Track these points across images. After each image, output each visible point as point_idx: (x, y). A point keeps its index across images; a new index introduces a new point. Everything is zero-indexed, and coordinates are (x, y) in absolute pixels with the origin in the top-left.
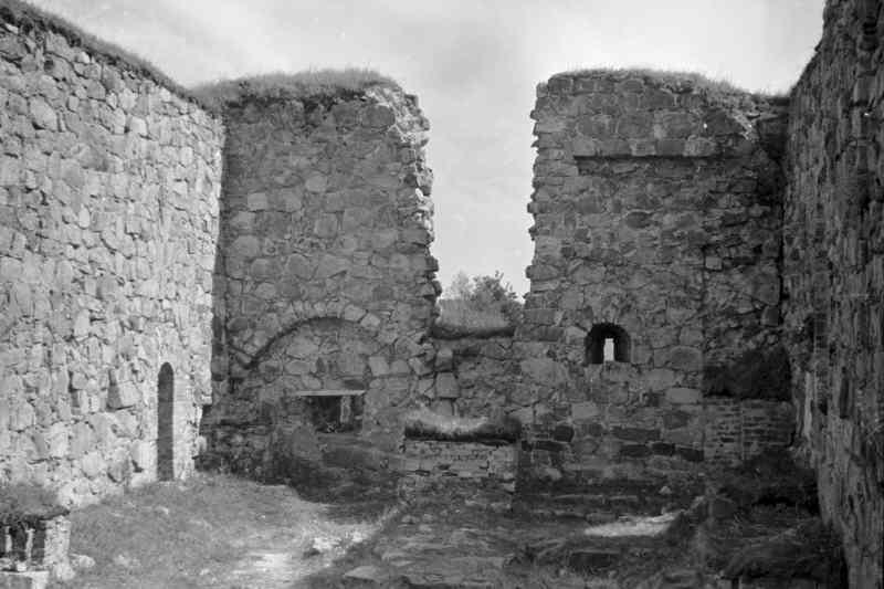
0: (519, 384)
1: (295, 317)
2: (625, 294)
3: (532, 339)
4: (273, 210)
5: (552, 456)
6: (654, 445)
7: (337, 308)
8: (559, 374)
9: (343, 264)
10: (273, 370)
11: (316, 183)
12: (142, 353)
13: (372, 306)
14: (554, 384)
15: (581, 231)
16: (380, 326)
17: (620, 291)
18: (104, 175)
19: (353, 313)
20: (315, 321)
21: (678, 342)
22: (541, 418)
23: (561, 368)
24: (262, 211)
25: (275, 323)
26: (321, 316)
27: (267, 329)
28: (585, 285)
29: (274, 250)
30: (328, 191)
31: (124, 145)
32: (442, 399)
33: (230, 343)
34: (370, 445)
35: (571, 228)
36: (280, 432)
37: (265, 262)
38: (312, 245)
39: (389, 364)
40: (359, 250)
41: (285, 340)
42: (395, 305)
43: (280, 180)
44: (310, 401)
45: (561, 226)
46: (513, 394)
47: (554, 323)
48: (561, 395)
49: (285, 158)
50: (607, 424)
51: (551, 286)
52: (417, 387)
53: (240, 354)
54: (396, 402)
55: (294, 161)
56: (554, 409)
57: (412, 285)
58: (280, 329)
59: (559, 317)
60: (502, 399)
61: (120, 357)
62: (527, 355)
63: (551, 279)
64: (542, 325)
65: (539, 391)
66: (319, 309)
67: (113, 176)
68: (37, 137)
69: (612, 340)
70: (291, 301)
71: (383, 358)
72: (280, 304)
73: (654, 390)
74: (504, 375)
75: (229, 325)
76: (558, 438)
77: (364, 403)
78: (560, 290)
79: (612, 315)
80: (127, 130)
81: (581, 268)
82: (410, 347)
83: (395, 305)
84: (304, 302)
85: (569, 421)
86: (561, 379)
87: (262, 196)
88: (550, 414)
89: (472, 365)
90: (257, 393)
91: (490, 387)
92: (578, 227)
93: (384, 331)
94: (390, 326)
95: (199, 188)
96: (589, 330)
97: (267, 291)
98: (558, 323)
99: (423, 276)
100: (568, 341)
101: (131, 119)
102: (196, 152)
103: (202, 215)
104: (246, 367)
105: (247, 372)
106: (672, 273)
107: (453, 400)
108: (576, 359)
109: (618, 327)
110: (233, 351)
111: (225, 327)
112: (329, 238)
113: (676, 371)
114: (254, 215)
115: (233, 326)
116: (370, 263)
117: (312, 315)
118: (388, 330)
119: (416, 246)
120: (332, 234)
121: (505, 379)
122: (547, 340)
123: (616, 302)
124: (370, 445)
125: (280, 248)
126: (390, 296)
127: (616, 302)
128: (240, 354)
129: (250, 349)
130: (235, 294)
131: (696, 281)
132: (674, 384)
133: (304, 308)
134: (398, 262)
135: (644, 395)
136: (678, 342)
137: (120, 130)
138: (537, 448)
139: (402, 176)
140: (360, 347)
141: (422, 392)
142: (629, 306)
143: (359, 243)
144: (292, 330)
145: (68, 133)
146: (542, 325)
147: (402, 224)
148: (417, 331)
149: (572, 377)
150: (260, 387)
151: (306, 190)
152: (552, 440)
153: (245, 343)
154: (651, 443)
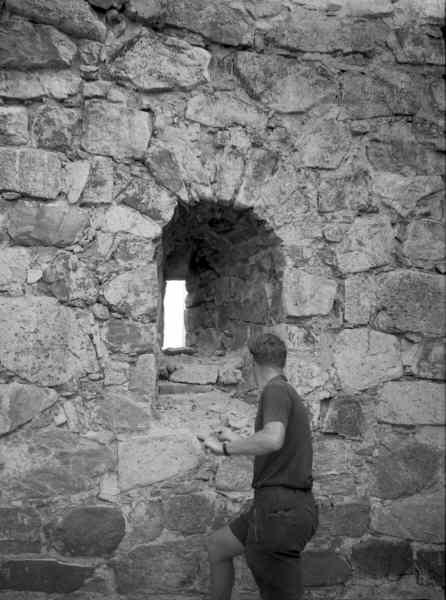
2: (263, 124)
6: (356, 553)
8: (77, 343)
14: (64, 378)
17: (251, 116)
21: (399, 261)
28: (154, 92)
50: (221, 491)
51: (59, 85)
56: (62, 455)
63: (57, 66)
65: (18, 393)
69: (182, 284)
73: (353, 384)
76: (73, 548)
79: (231, 178)
81: (145, 41)
85: (109, 489)
86: (77, 364)
96: (168, 215)
98: (74, 197)
100: (104, 246)
106: (380, 80)
108: (131, 300)
109: (246, 213)
113: (399, 334)
123: (242, 141)
127: (242, 141)
131: (433, 104)
132: (397, 371)
135: (326, 401)
136: (399, 261)
142: (276, 157)
146: (25, 196)
149: (113, 351)
152: (52, 556)
154: (349, 543)
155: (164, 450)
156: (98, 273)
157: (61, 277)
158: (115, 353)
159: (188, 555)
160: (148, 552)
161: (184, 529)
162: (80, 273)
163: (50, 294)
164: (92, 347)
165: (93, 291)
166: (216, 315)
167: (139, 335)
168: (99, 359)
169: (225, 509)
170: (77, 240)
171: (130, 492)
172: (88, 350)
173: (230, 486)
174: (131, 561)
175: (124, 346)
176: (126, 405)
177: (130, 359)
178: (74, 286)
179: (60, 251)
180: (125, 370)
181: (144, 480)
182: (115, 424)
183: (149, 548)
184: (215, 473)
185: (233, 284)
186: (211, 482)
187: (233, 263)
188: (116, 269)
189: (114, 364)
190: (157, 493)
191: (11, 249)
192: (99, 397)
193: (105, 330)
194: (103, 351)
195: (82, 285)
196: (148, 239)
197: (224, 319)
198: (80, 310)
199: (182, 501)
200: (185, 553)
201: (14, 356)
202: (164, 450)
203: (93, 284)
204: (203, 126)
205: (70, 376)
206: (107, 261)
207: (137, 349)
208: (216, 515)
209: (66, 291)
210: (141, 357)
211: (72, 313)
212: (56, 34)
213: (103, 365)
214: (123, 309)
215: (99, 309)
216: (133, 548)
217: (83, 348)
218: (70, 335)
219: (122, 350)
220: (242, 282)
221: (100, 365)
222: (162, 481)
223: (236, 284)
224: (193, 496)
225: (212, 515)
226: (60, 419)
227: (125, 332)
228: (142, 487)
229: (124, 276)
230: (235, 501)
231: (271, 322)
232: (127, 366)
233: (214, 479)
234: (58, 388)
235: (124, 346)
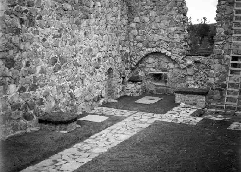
1: (148, 52)
3: (215, 58)
4: (141, 22)
5: (220, 92)
7: (159, 49)
8: (222, 69)
9: (161, 37)
10: (143, 67)
11: (153, 13)
12: (102, 66)
13: (169, 49)
15: (230, 26)
16: (171, 54)
18: (87, 20)
19: (164, 51)
20: (153, 53)
22: (217, 81)
24: (138, 22)
25: (143, 54)
26: (155, 52)
27: (140, 55)
29: (142, 33)
30: (156, 16)
31: (93, 10)
32: (189, 75)
33: (131, 59)
34: (169, 87)
35: (227, 25)
36: (145, 84)
37: (139, 37)
38: (152, 32)
40: (165, 33)
41: (145, 58)
42: (175, 49)
43: (143, 13)
44: (153, 75)
45: (224, 25)
46: (209, 74)
47: (222, 54)
48: (223, 75)
49: (144, 7)
51: (221, 43)
52: (182, 72)
53: (134, 63)
55: (146, 7)
56: (221, 79)
57: (180, 43)
58: (144, 55)
59: (223, 52)
61: (95, 69)
62: (213, 63)
63: (221, 41)
64: (218, 54)
66: (154, 50)
67: (90, 20)
68: (66, 13)
70: (147, 47)
71: (172, 63)
72: (144, 49)
75: (130, 54)
77: (167, 76)
78: (223, 44)
80: (94, 6)
82: (179, 61)
83: (175, 49)
84: (150, 48)
85: (225, 82)
87: (138, 18)
88: (219, 80)
90: (139, 73)
92: (229, 25)
93: (172, 57)
94: (174, 55)
95: (119, 18)
97: (140, 45)
98: (223, 54)
99: (183, 40)
101: (95, 2)
102: (118, 8)
103: (120, 25)
104: (135, 66)
105: (136, 67)
108: (228, 64)
110: (132, 61)
111: (130, 55)
112: (157, 30)
114: (136, 24)
115: (131, 54)
116: (168, 37)
117: (152, 51)
118: (174, 56)
119: (181, 32)
120: (158, 28)
124: (169, 87)
125: (143, 33)
126: (174, 46)
128: (134, 63)
129: (137, 61)
130: (132, 46)
133: (150, 49)
134: (176, 36)
137: (92, 6)
138: (215, 89)
139: (177, 11)
140: (166, 60)
141: (183, 73)
143: (165, 31)
144: (147, 55)
145: (75, 11)
146: (218, 54)
147: (177, 25)
148: (182, 56)
149: (226, 69)
150: (139, 71)
151: (150, 16)
152: (220, 88)
153: (135, 59)
204: (236, 46)
209: (222, 63)
212: (221, 37)
215: (225, 65)
226: (221, 75)
229: (227, 62)
234: (221, 73)
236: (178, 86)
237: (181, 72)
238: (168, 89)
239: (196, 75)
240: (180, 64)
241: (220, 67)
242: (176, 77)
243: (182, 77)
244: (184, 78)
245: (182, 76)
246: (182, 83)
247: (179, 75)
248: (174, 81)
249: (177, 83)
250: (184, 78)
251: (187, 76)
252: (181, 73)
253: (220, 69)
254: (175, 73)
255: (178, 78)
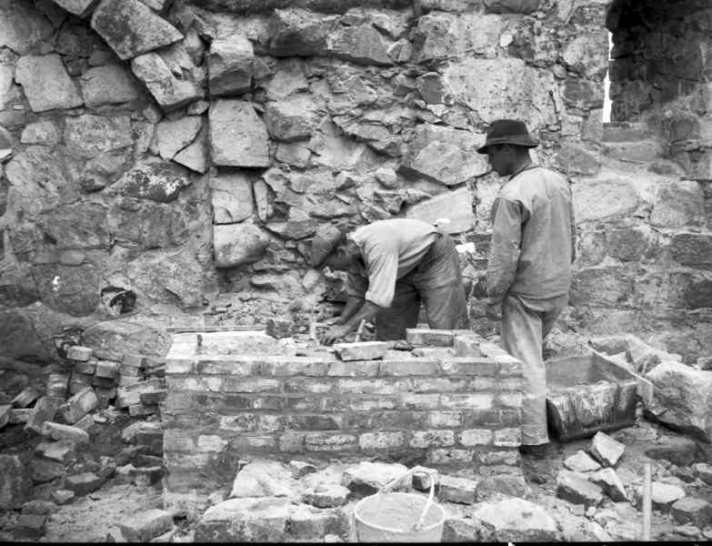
0: (434, 128)
8: (538, 100)
23: (548, 84)
39: (75, 76)
50: (655, 228)
52: (155, 140)
54: (98, 182)
60: (388, 171)
62: (460, 47)
71: (55, 59)
74: (386, 106)
89: (302, 84)
91: (353, 139)
107: (253, 173)
108: (586, 61)
121: (391, 118)
122: (511, 10)
141: (167, 153)
149: (569, 106)
155: (609, 191)
156: (558, 37)
157: (527, 41)
158: (571, 107)
159: (624, 278)
160: (594, 274)
161: (622, 257)
162: (543, 38)
163: (519, 56)
164: (551, 102)
165: (553, 53)
166: (644, 68)
167: (592, 93)
168: (556, 113)
169: (658, 242)
170: (540, 7)
171: (580, 226)
172: (548, 105)
173: (662, 223)
174: (579, 281)
175: (578, 101)
176: (579, 153)
177: (582, 113)
178: (537, 49)
179: (526, 17)
180: (578, 123)
181: (591, 214)
182: (571, 169)
183: (593, 270)
184: (650, 212)
185: (664, 40)
186: (646, 220)
187: (666, 18)
188: (574, 33)
189: (570, 117)
190: (602, 227)
191: (486, 17)
192: (557, 147)
193: (563, 88)
194: (560, 106)
195: (545, 48)
196: (602, 5)
197: (654, 70)
198: (542, 70)
199: (621, 233)
200: (623, 276)
201: (490, 110)
202: (609, 191)
203: (553, 47)
205: (533, 128)
206: (566, 26)
207: (589, 105)
208: (650, 245)
209: (532, 53)
210: (592, 112)
211: (536, 72)
213: (560, 118)
214: (579, 70)
215: (558, 69)
216: (582, 270)
217: (543, 104)
218: (534, 91)
219: (577, 106)
220: (674, 38)
221: (557, 118)
222: (606, 217)
223: (669, 40)
224: (632, 230)
225: (646, 246)
227: (579, 89)
228: (590, 221)
229: (580, 40)
230: (666, 236)
231: (704, 79)
232: (580, 119)
233: (649, 217)
235: (578, 101)
236: (118, 282)
237: (142, 144)
238: (21, 312)
239: (295, 168)
240: (140, 60)
241: (515, 91)
242: (98, 190)
243: (159, 196)
244: (173, 198)
245: (154, 180)
246: (155, 248)
247: (127, 179)
248: (84, 235)
249: (110, 249)
250: (173, 198)
251: (200, 187)
252: (149, 152)
253: (523, 107)
254: (85, 159)
255: (119, 200)
